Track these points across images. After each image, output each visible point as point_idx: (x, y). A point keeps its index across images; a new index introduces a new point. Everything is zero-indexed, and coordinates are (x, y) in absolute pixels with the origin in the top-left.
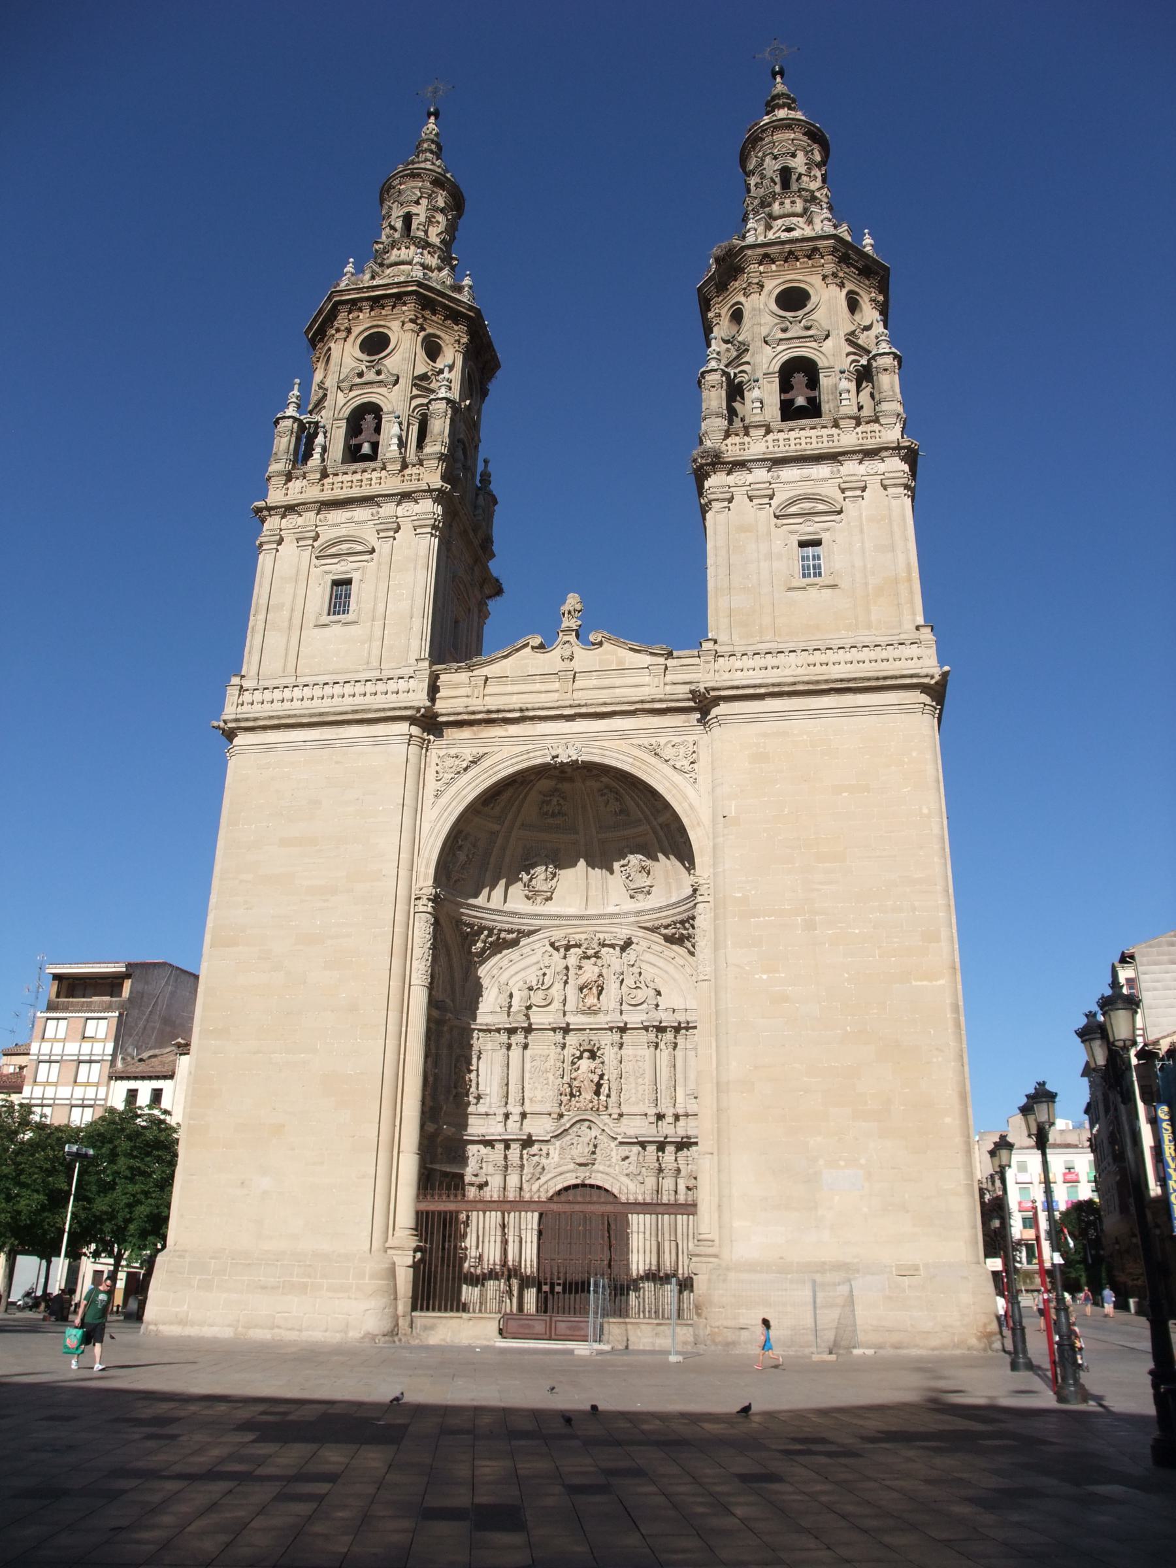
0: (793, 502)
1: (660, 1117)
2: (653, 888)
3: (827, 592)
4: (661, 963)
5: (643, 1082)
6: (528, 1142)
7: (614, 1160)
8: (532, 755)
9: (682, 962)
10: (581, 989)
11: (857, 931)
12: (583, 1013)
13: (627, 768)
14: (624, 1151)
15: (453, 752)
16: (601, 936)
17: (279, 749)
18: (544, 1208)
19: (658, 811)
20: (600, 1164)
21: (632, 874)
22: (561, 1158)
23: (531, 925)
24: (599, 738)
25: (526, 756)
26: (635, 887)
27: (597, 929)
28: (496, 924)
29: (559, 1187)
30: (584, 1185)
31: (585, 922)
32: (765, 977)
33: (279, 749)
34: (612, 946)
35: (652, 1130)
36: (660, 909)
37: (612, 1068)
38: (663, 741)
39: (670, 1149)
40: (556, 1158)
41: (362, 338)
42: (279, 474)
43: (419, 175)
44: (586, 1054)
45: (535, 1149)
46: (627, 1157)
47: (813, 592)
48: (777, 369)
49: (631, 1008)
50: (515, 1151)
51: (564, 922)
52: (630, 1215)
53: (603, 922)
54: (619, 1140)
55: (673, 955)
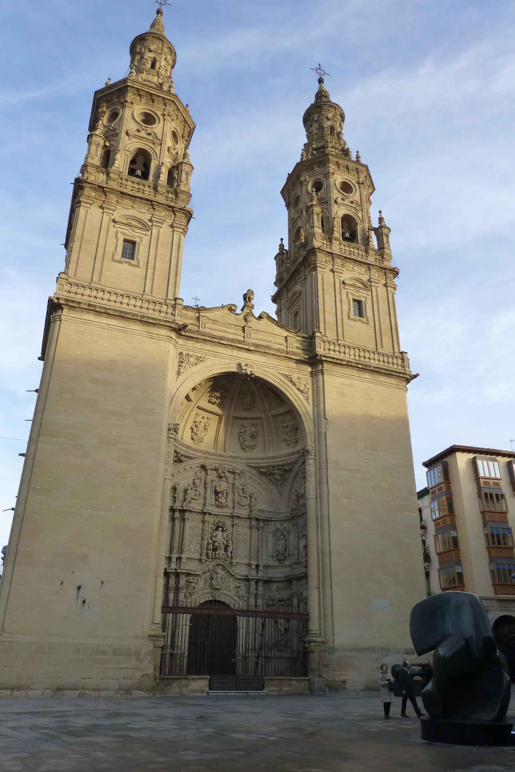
0: (352, 279)
1: (257, 566)
2: (256, 447)
3: (365, 326)
4: (255, 485)
5: (247, 547)
6: (188, 574)
7: (231, 588)
8: (231, 365)
9: (265, 486)
10: (217, 493)
11: (383, 485)
12: (218, 506)
13: (276, 384)
14: (237, 583)
15: (191, 353)
16: (230, 467)
17: (91, 325)
18: (195, 611)
19: (272, 409)
20: (225, 589)
21: (247, 438)
22: (204, 585)
23: (195, 455)
24: (264, 366)
25: (228, 366)
26: (246, 444)
27: (226, 463)
28: (181, 451)
29: (202, 601)
30: (215, 601)
31: (220, 458)
32: (346, 501)
33: (91, 325)
34: (234, 473)
35: (254, 573)
36: (263, 459)
37: (233, 538)
38: (294, 375)
39: (260, 584)
40: (202, 585)
41: (148, 111)
42: (93, 166)
43: (162, 40)
44: (220, 529)
45: (191, 578)
46: (240, 587)
47: (359, 324)
48: (340, 216)
49: (241, 507)
50: (182, 580)
51: (210, 456)
52: (238, 618)
53: (229, 459)
54: (237, 577)
55: (262, 482)
